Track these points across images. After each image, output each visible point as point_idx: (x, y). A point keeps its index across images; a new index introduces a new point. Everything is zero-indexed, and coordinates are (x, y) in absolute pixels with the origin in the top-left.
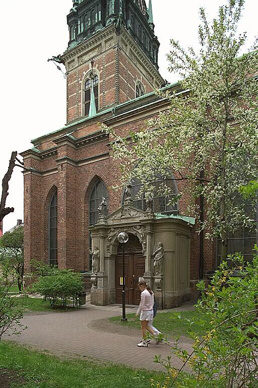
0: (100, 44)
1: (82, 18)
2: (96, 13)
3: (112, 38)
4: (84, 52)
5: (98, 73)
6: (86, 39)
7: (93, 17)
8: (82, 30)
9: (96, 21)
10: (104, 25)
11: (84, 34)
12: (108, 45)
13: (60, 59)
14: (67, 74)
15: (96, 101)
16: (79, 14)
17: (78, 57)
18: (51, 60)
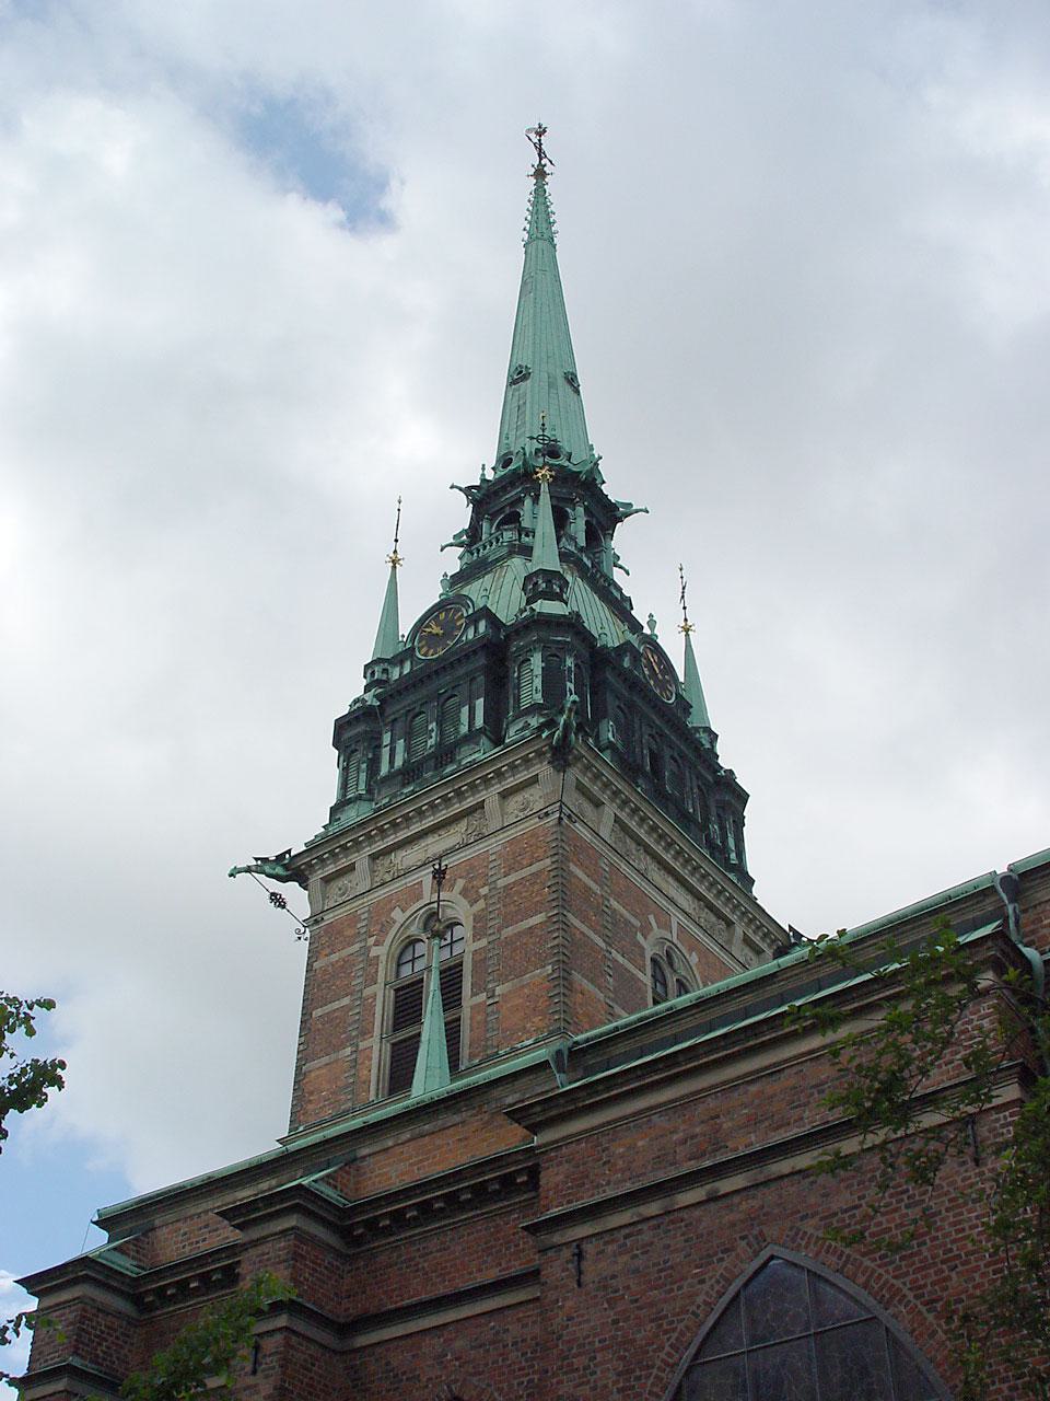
0: (481, 805)
1: (399, 725)
2: (460, 705)
4: (402, 835)
6: (413, 792)
8: (399, 762)
10: (498, 740)
11: (410, 773)
12: (515, 803)
14: (314, 920)
15: (452, 1032)
16: (389, 711)
17: (374, 857)
18: (248, 870)
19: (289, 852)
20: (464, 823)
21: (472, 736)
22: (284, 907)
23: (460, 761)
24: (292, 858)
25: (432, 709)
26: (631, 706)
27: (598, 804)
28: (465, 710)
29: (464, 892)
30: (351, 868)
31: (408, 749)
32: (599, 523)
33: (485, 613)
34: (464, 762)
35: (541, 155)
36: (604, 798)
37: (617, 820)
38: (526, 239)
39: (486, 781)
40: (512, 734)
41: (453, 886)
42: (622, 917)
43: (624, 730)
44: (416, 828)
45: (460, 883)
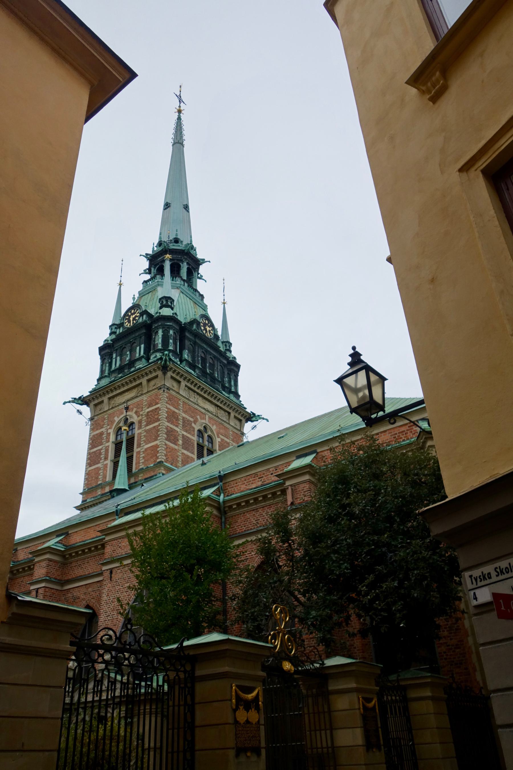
1: (118, 351)
2: (137, 346)
3: (157, 377)
4: (118, 391)
5: (135, 419)
6: (122, 377)
7: (132, 351)
8: (118, 365)
9: (137, 355)
10: (148, 359)
12: (152, 383)
13: (83, 401)
14: (91, 419)
16: (115, 346)
17: (110, 399)
18: (69, 402)
19: (83, 396)
20: (137, 389)
21: (140, 359)
22: (81, 414)
23: (136, 367)
24: (84, 398)
25: (128, 347)
26: (195, 343)
27: (179, 382)
28: (138, 348)
29: (136, 413)
30: (102, 402)
31: (121, 360)
32: (192, 267)
33: (146, 312)
34: (137, 367)
35: (180, 101)
36: (181, 380)
37: (186, 386)
38: (173, 142)
39: (143, 376)
40: (152, 358)
41: (132, 410)
42: (186, 419)
43: (193, 353)
44: (122, 389)
45: (135, 410)
